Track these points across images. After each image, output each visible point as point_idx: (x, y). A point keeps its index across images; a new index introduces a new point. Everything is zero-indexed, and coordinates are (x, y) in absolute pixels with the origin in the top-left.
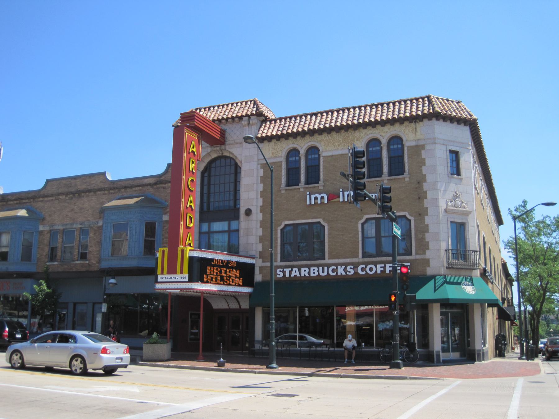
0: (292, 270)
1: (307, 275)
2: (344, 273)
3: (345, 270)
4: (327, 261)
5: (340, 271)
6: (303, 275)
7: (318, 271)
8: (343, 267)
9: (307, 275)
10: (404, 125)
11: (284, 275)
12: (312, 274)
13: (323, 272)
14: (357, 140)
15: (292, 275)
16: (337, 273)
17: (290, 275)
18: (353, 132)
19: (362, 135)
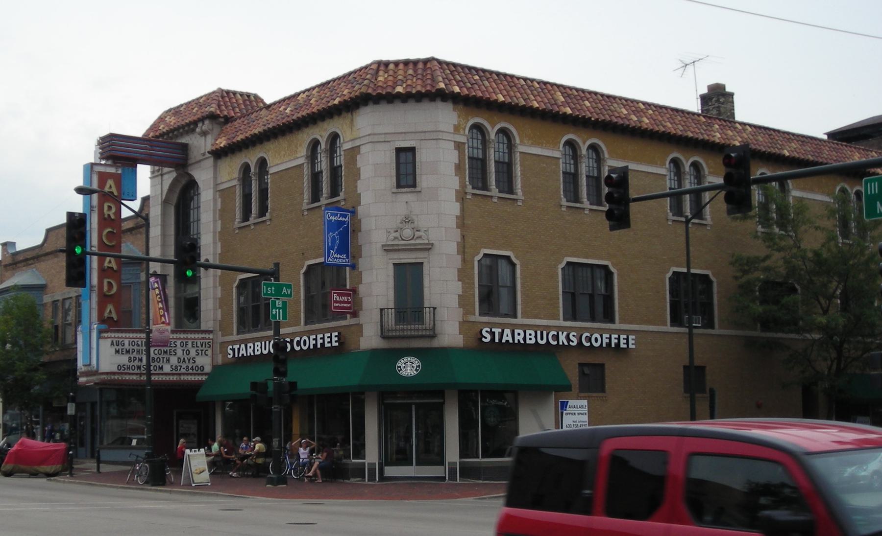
0: (503, 331)
2: (566, 343)
3: (568, 337)
6: (516, 341)
7: (536, 337)
8: (565, 333)
12: (528, 342)
13: (542, 339)
15: (504, 341)
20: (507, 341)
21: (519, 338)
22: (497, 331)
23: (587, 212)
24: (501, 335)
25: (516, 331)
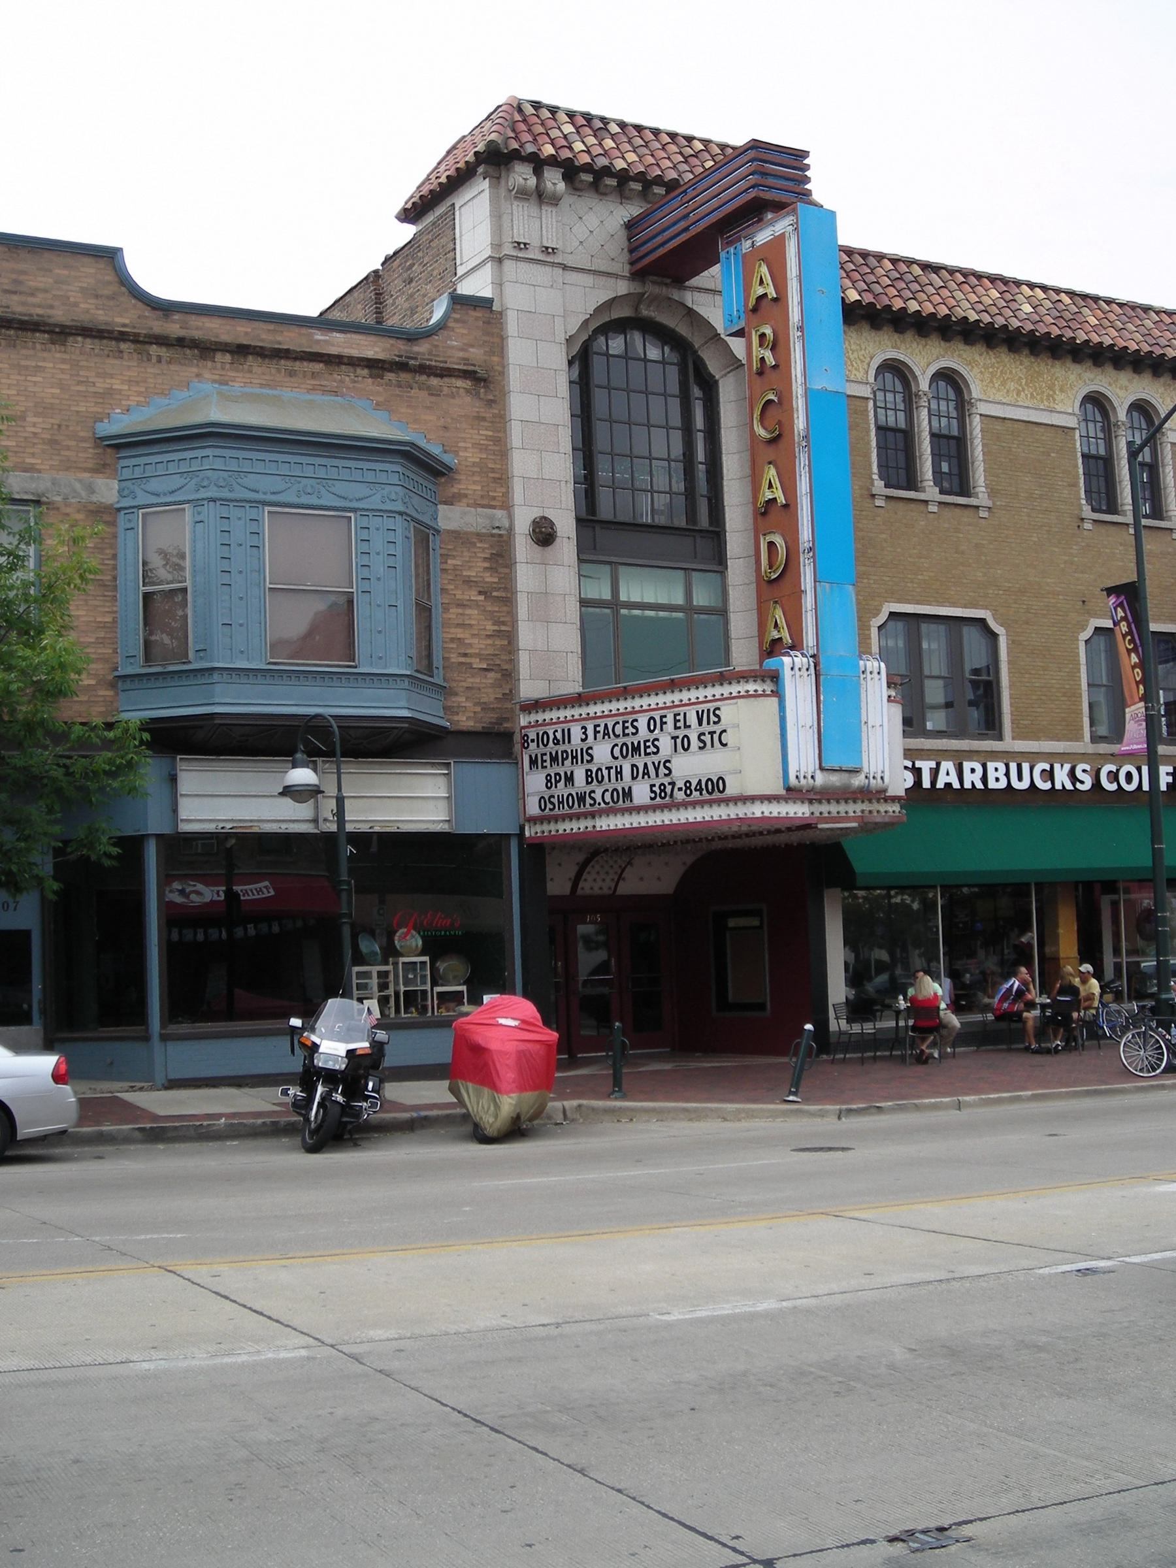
0: (938, 764)
1: (979, 785)
2: (1069, 786)
3: (1072, 775)
4: (1009, 743)
5: (1062, 778)
6: (968, 785)
7: (1007, 774)
8: (1067, 767)
9: (979, 785)
10: (1162, 380)
11: (918, 782)
12: (992, 785)
13: (1020, 778)
14: (1062, 390)
15: (940, 785)
16: (1053, 784)
17: (934, 782)
18: (1050, 362)
19: (1073, 377)
20: (948, 785)
21: (972, 779)
22: (926, 766)
23: (933, 508)
24: (935, 773)
25: (967, 766)
